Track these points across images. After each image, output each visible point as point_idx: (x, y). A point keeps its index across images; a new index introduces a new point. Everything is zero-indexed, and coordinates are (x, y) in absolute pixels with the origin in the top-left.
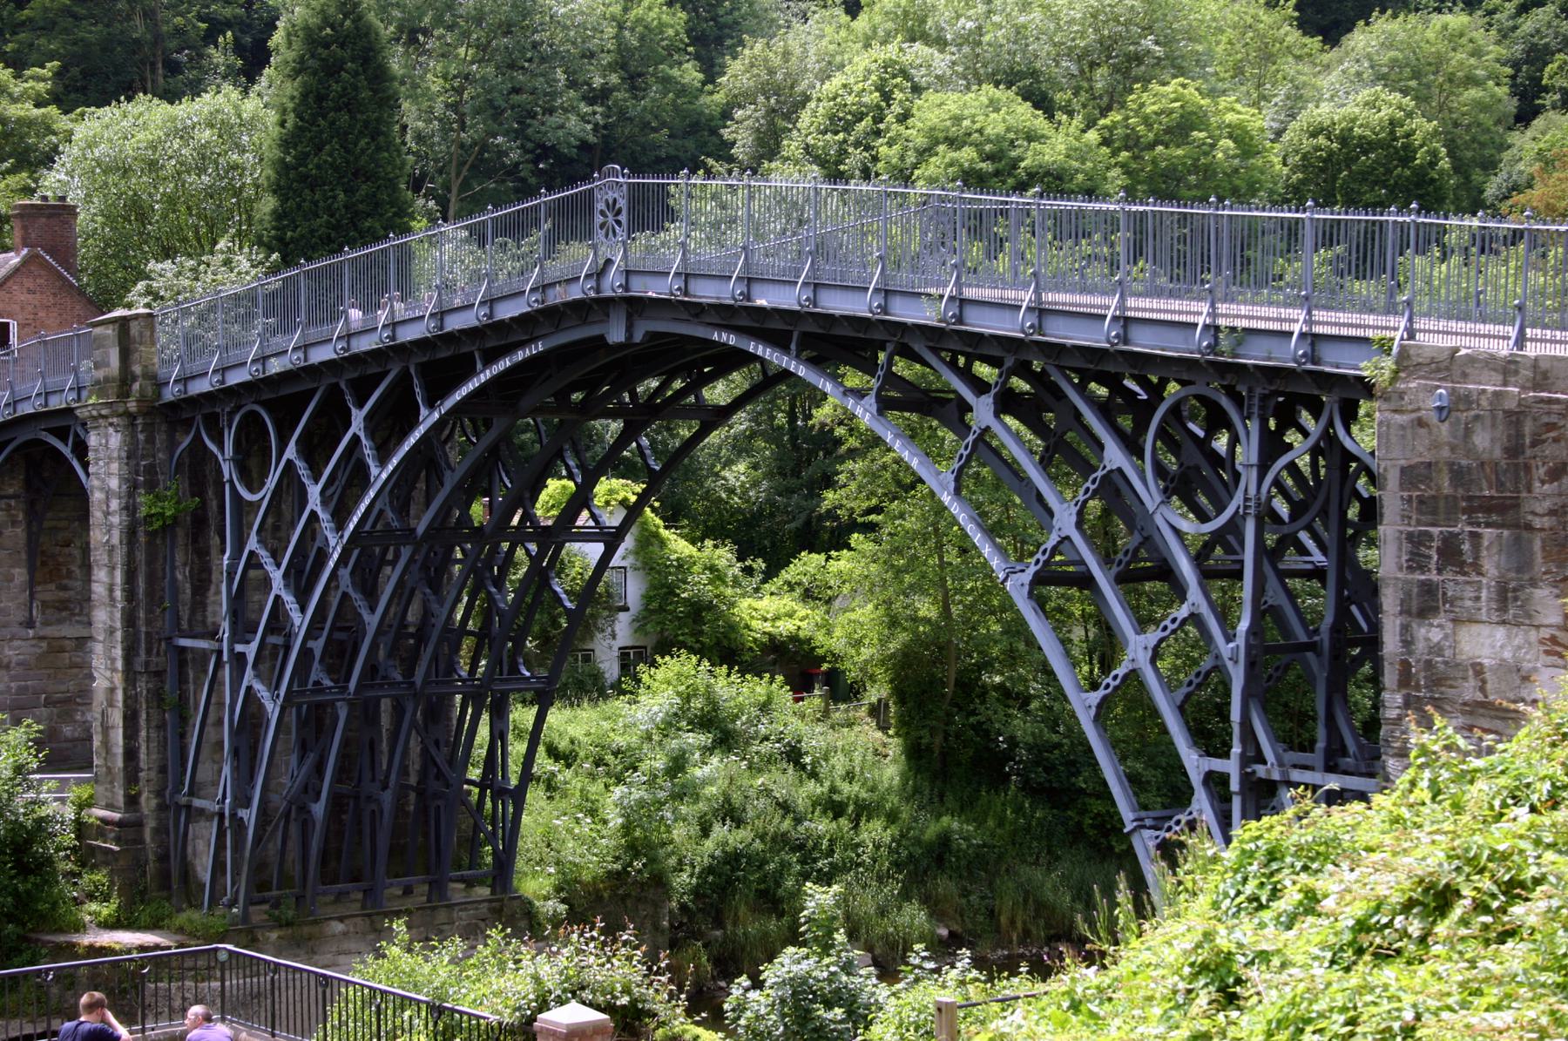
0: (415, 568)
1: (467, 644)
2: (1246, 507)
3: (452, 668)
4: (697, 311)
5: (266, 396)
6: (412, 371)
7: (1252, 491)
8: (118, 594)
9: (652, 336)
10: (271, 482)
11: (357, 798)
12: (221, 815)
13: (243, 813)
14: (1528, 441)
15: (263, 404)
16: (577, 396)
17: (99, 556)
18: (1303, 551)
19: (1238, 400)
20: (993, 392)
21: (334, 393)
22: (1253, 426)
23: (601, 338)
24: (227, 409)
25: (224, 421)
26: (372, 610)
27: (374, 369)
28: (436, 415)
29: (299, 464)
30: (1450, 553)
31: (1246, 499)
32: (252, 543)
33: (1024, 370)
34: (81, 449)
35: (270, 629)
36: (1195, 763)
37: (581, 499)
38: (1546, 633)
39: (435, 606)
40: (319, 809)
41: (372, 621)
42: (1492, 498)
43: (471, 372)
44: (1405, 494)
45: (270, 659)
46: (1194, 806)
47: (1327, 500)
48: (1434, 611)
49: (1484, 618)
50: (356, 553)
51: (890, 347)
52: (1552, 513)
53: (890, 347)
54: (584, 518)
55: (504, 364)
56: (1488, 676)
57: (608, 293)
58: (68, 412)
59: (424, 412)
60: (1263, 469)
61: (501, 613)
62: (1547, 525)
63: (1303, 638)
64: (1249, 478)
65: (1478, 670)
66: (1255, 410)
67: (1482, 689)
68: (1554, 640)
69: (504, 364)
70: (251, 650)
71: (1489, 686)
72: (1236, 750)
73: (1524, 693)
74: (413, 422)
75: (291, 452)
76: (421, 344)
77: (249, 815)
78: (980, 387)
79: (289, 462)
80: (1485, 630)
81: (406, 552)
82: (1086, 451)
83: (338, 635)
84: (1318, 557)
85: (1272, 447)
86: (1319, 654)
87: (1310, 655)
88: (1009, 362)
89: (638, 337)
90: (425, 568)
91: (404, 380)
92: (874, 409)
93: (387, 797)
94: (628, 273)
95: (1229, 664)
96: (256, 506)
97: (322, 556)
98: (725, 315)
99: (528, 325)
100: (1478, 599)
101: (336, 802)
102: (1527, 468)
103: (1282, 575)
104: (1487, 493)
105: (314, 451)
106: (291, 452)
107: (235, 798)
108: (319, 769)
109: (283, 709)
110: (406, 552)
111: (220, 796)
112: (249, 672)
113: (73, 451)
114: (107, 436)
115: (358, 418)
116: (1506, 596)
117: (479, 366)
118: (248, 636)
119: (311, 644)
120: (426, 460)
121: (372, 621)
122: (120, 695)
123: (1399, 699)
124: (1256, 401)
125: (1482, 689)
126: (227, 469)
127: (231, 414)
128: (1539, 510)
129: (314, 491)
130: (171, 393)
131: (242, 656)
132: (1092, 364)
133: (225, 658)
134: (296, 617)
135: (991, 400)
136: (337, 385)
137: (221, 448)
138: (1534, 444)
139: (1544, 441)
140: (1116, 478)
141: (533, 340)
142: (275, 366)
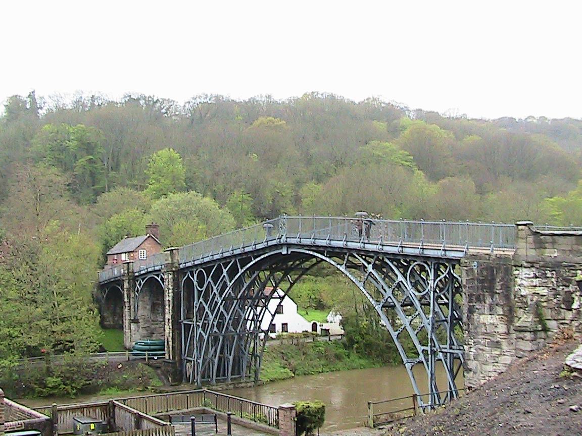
0: (237, 305)
1: (249, 322)
3: (245, 328)
4: (303, 246)
6: (237, 260)
7: (432, 286)
8: (171, 311)
9: (292, 252)
10: (205, 286)
11: (224, 357)
12: (194, 361)
13: (198, 361)
15: (203, 268)
16: (273, 266)
17: (167, 303)
18: (442, 299)
21: (219, 266)
22: (433, 270)
23: (281, 253)
24: (195, 270)
25: (194, 273)
26: (228, 315)
27: (228, 260)
28: (243, 271)
29: (212, 282)
32: (201, 300)
33: (378, 259)
34: (162, 279)
35: (204, 320)
36: (420, 348)
37: (274, 291)
39: (242, 314)
40: (216, 360)
41: (228, 318)
45: (204, 327)
46: (420, 357)
47: (448, 288)
50: (224, 302)
51: (348, 254)
53: (348, 254)
54: (276, 295)
55: (259, 259)
56: (487, 326)
57: (282, 241)
58: (159, 270)
59: (240, 269)
60: (434, 281)
61: (257, 315)
63: (444, 319)
64: (431, 282)
65: (485, 324)
69: (259, 259)
70: (200, 324)
71: (487, 329)
72: (429, 344)
75: (210, 279)
76: (240, 254)
77: (200, 361)
78: (369, 263)
79: (209, 282)
80: (486, 316)
81: (235, 301)
82: (393, 277)
83: (220, 321)
84: (446, 301)
85: (436, 276)
86: (448, 323)
87: (445, 323)
88: (375, 257)
89: (289, 253)
90: (239, 305)
91: (235, 263)
93: (231, 358)
94: (287, 238)
95: (428, 325)
96: (203, 291)
97: (216, 303)
98: (309, 247)
99: (264, 250)
100: (484, 309)
101: (220, 359)
103: (439, 304)
105: (215, 279)
106: (210, 279)
107: (197, 358)
108: (216, 351)
109: (208, 338)
110: (235, 301)
111: (193, 357)
112: (200, 329)
113: (161, 279)
114: (168, 276)
115: (225, 273)
116: (491, 308)
117: (253, 259)
118: (200, 321)
119: (214, 323)
120: (240, 282)
121: (228, 318)
122: (171, 334)
126: (195, 283)
128: (498, 288)
129: (215, 288)
130: (181, 266)
131: (199, 325)
132: (394, 257)
133: (195, 325)
134: (211, 316)
136: (220, 264)
137: (193, 277)
140: (400, 283)
142: (206, 260)
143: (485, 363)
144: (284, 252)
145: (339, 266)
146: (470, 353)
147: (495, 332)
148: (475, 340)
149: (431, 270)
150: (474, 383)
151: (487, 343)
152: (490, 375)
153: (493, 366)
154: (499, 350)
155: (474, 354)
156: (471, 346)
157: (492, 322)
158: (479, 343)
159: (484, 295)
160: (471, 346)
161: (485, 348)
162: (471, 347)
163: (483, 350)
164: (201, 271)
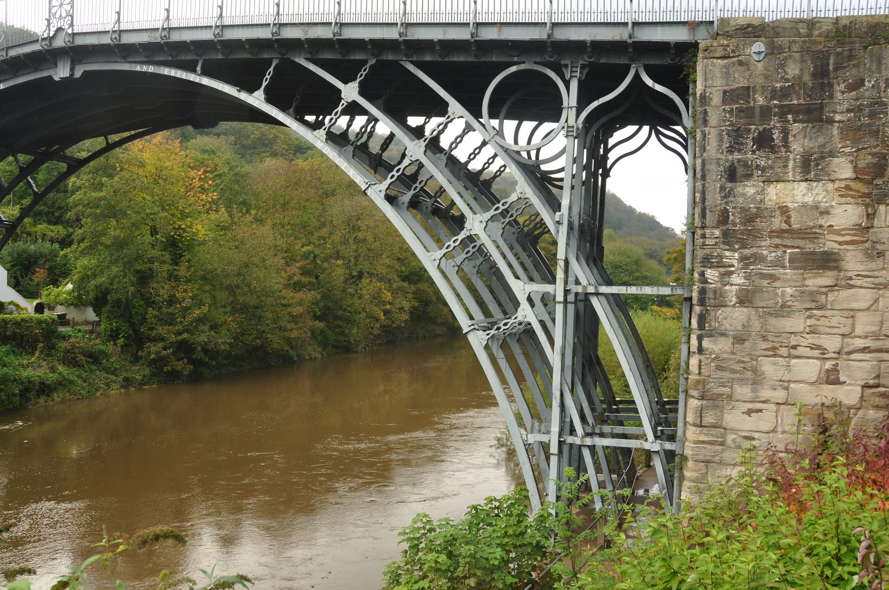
14: (831, 68)
20: (358, 80)
22: (574, 85)
30: (764, 141)
38: (837, 184)
42: (800, 105)
44: (727, 108)
48: (748, 176)
49: (791, 178)
52: (849, 111)
56: (792, 214)
62: (845, 119)
65: (784, 210)
66: (578, 74)
67: (787, 222)
68: (848, 188)
71: (792, 219)
73: (821, 222)
80: (789, 186)
89: (78, 74)
92: (263, 97)
100: (786, 166)
102: (830, 85)
104: (795, 102)
123: (717, 232)
125: (787, 222)
135: (357, 85)
138: (836, 69)
139: (845, 67)
143: (784, 310)
144: (61, 72)
145: (244, 96)
146: (727, 287)
147: (821, 226)
148: (746, 252)
150: (737, 367)
151: (787, 257)
152: (793, 343)
153: (810, 317)
154: (831, 273)
155: (741, 290)
156: (732, 269)
157: (809, 199)
158: (759, 259)
159: (785, 133)
160: (732, 269)
161: (782, 271)
162: (732, 273)
163: (773, 278)
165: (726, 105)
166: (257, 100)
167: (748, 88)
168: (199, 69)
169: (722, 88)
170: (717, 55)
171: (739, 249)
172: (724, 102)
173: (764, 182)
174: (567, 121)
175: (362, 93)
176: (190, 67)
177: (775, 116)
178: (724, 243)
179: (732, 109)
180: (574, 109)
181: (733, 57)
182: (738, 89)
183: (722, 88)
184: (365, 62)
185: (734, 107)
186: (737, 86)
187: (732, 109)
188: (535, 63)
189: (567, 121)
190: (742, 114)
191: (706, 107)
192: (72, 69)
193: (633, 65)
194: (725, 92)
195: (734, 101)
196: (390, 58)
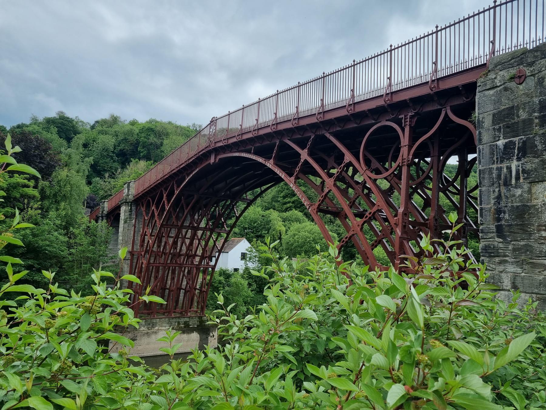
2: (402, 163)
5: (151, 195)
7: (405, 156)
19: (399, 123)
20: (307, 147)
21: (162, 191)
22: (407, 130)
31: (403, 159)
43: (185, 179)
44: (497, 127)
64: (404, 151)
66: (408, 123)
74: (174, 194)
124: (408, 120)
127: (145, 200)
135: (307, 150)
141: (196, 168)
144: (212, 160)
149: (403, 130)
164: (149, 200)
165: (495, 125)
166: (270, 164)
167: (513, 107)
168: (252, 152)
169: (492, 112)
170: (488, 87)
171: (511, 241)
172: (494, 123)
173: (530, 183)
174: (403, 156)
175: (310, 154)
176: (249, 152)
177: (536, 126)
178: (499, 237)
179: (500, 127)
180: (407, 146)
181: (501, 86)
182: (504, 110)
183: (492, 112)
184: (310, 137)
185: (501, 125)
186: (503, 107)
187: (500, 127)
188: (387, 120)
189: (403, 156)
190: (508, 130)
191: (480, 130)
192: (215, 158)
193: (443, 109)
194: (494, 115)
195: (502, 121)
196: (320, 133)
